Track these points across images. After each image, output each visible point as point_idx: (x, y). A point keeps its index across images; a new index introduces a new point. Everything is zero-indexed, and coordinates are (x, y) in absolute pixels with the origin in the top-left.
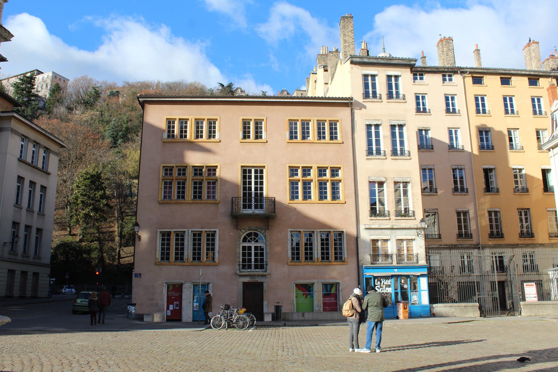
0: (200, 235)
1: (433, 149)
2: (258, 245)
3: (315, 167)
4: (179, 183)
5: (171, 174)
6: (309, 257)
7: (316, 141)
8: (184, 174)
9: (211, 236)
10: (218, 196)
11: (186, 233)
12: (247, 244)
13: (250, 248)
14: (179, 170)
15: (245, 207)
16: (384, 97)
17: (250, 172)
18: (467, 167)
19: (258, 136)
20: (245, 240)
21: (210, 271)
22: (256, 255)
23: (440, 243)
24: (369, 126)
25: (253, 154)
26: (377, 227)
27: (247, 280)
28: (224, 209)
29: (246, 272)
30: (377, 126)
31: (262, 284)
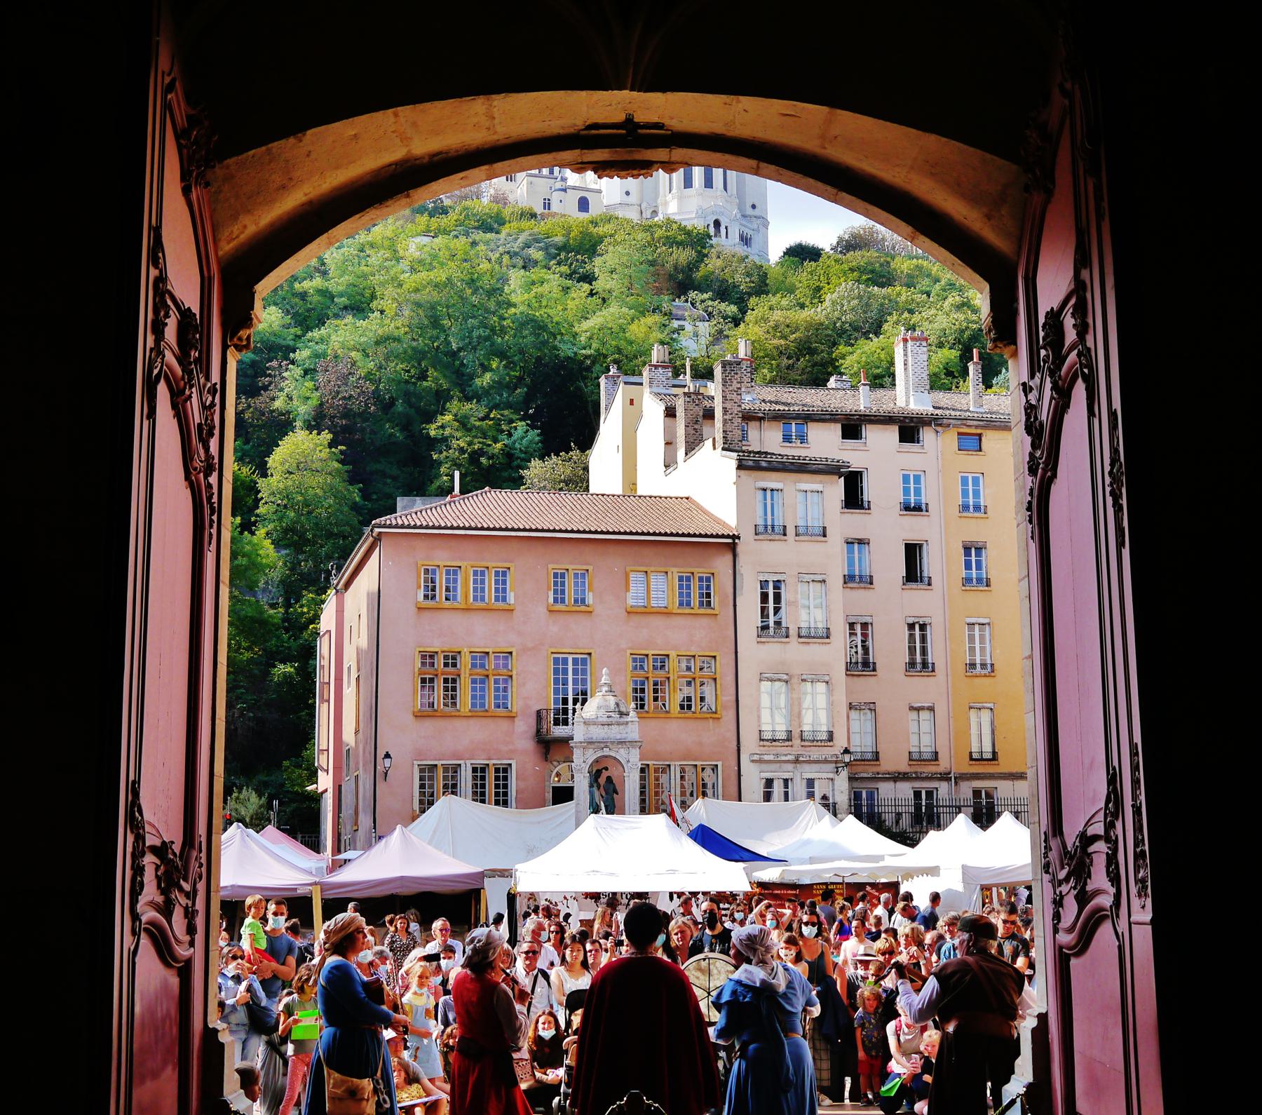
0: (483, 770)
1: (871, 583)
4: (446, 681)
5: (432, 664)
8: (454, 665)
10: (516, 704)
11: (463, 768)
14: (446, 657)
15: (557, 723)
17: (565, 661)
23: (875, 769)
25: (575, 635)
26: (771, 758)
28: (524, 728)
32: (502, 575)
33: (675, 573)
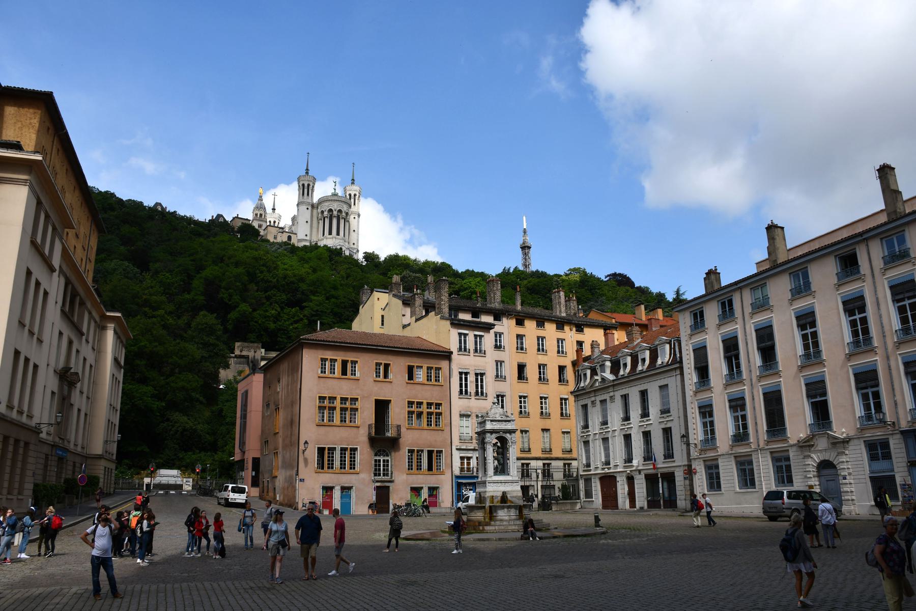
2: (386, 458)
3: (425, 402)
6: (419, 467)
7: (426, 382)
9: (354, 450)
12: (378, 458)
13: (380, 461)
16: (472, 351)
18: (508, 394)
19: (386, 376)
20: (376, 455)
21: (354, 476)
22: (384, 466)
24: (461, 373)
27: (378, 484)
29: (377, 478)
30: (466, 374)
31: (389, 487)
32: (354, 363)
33: (425, 367)
